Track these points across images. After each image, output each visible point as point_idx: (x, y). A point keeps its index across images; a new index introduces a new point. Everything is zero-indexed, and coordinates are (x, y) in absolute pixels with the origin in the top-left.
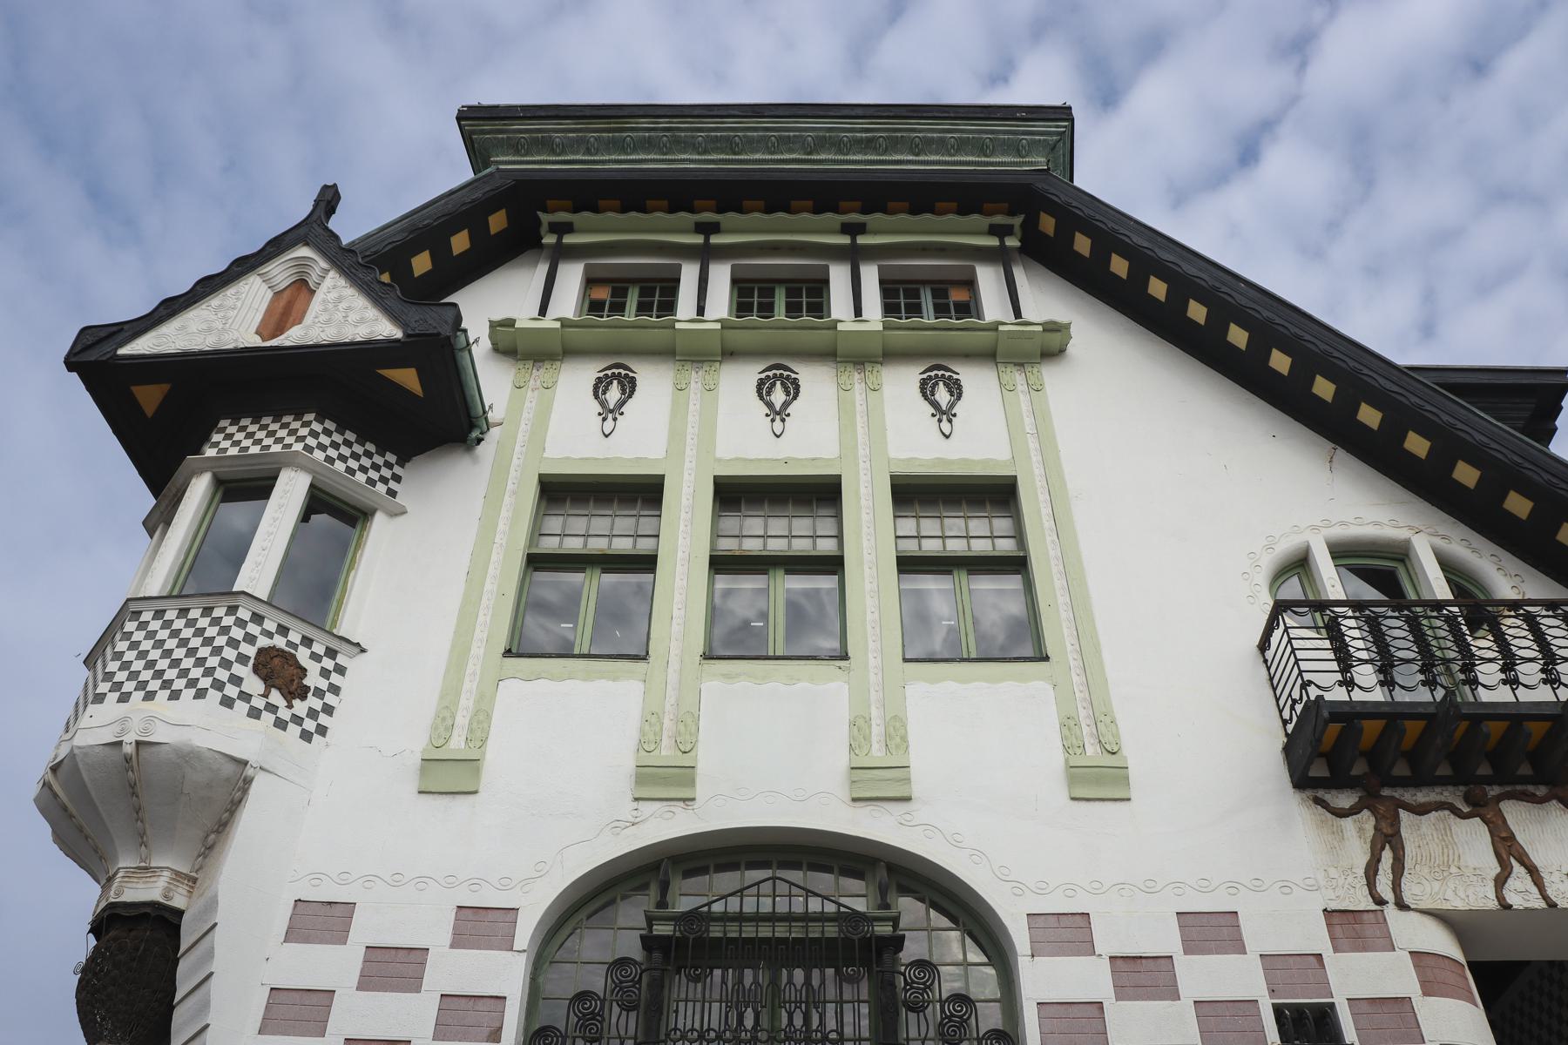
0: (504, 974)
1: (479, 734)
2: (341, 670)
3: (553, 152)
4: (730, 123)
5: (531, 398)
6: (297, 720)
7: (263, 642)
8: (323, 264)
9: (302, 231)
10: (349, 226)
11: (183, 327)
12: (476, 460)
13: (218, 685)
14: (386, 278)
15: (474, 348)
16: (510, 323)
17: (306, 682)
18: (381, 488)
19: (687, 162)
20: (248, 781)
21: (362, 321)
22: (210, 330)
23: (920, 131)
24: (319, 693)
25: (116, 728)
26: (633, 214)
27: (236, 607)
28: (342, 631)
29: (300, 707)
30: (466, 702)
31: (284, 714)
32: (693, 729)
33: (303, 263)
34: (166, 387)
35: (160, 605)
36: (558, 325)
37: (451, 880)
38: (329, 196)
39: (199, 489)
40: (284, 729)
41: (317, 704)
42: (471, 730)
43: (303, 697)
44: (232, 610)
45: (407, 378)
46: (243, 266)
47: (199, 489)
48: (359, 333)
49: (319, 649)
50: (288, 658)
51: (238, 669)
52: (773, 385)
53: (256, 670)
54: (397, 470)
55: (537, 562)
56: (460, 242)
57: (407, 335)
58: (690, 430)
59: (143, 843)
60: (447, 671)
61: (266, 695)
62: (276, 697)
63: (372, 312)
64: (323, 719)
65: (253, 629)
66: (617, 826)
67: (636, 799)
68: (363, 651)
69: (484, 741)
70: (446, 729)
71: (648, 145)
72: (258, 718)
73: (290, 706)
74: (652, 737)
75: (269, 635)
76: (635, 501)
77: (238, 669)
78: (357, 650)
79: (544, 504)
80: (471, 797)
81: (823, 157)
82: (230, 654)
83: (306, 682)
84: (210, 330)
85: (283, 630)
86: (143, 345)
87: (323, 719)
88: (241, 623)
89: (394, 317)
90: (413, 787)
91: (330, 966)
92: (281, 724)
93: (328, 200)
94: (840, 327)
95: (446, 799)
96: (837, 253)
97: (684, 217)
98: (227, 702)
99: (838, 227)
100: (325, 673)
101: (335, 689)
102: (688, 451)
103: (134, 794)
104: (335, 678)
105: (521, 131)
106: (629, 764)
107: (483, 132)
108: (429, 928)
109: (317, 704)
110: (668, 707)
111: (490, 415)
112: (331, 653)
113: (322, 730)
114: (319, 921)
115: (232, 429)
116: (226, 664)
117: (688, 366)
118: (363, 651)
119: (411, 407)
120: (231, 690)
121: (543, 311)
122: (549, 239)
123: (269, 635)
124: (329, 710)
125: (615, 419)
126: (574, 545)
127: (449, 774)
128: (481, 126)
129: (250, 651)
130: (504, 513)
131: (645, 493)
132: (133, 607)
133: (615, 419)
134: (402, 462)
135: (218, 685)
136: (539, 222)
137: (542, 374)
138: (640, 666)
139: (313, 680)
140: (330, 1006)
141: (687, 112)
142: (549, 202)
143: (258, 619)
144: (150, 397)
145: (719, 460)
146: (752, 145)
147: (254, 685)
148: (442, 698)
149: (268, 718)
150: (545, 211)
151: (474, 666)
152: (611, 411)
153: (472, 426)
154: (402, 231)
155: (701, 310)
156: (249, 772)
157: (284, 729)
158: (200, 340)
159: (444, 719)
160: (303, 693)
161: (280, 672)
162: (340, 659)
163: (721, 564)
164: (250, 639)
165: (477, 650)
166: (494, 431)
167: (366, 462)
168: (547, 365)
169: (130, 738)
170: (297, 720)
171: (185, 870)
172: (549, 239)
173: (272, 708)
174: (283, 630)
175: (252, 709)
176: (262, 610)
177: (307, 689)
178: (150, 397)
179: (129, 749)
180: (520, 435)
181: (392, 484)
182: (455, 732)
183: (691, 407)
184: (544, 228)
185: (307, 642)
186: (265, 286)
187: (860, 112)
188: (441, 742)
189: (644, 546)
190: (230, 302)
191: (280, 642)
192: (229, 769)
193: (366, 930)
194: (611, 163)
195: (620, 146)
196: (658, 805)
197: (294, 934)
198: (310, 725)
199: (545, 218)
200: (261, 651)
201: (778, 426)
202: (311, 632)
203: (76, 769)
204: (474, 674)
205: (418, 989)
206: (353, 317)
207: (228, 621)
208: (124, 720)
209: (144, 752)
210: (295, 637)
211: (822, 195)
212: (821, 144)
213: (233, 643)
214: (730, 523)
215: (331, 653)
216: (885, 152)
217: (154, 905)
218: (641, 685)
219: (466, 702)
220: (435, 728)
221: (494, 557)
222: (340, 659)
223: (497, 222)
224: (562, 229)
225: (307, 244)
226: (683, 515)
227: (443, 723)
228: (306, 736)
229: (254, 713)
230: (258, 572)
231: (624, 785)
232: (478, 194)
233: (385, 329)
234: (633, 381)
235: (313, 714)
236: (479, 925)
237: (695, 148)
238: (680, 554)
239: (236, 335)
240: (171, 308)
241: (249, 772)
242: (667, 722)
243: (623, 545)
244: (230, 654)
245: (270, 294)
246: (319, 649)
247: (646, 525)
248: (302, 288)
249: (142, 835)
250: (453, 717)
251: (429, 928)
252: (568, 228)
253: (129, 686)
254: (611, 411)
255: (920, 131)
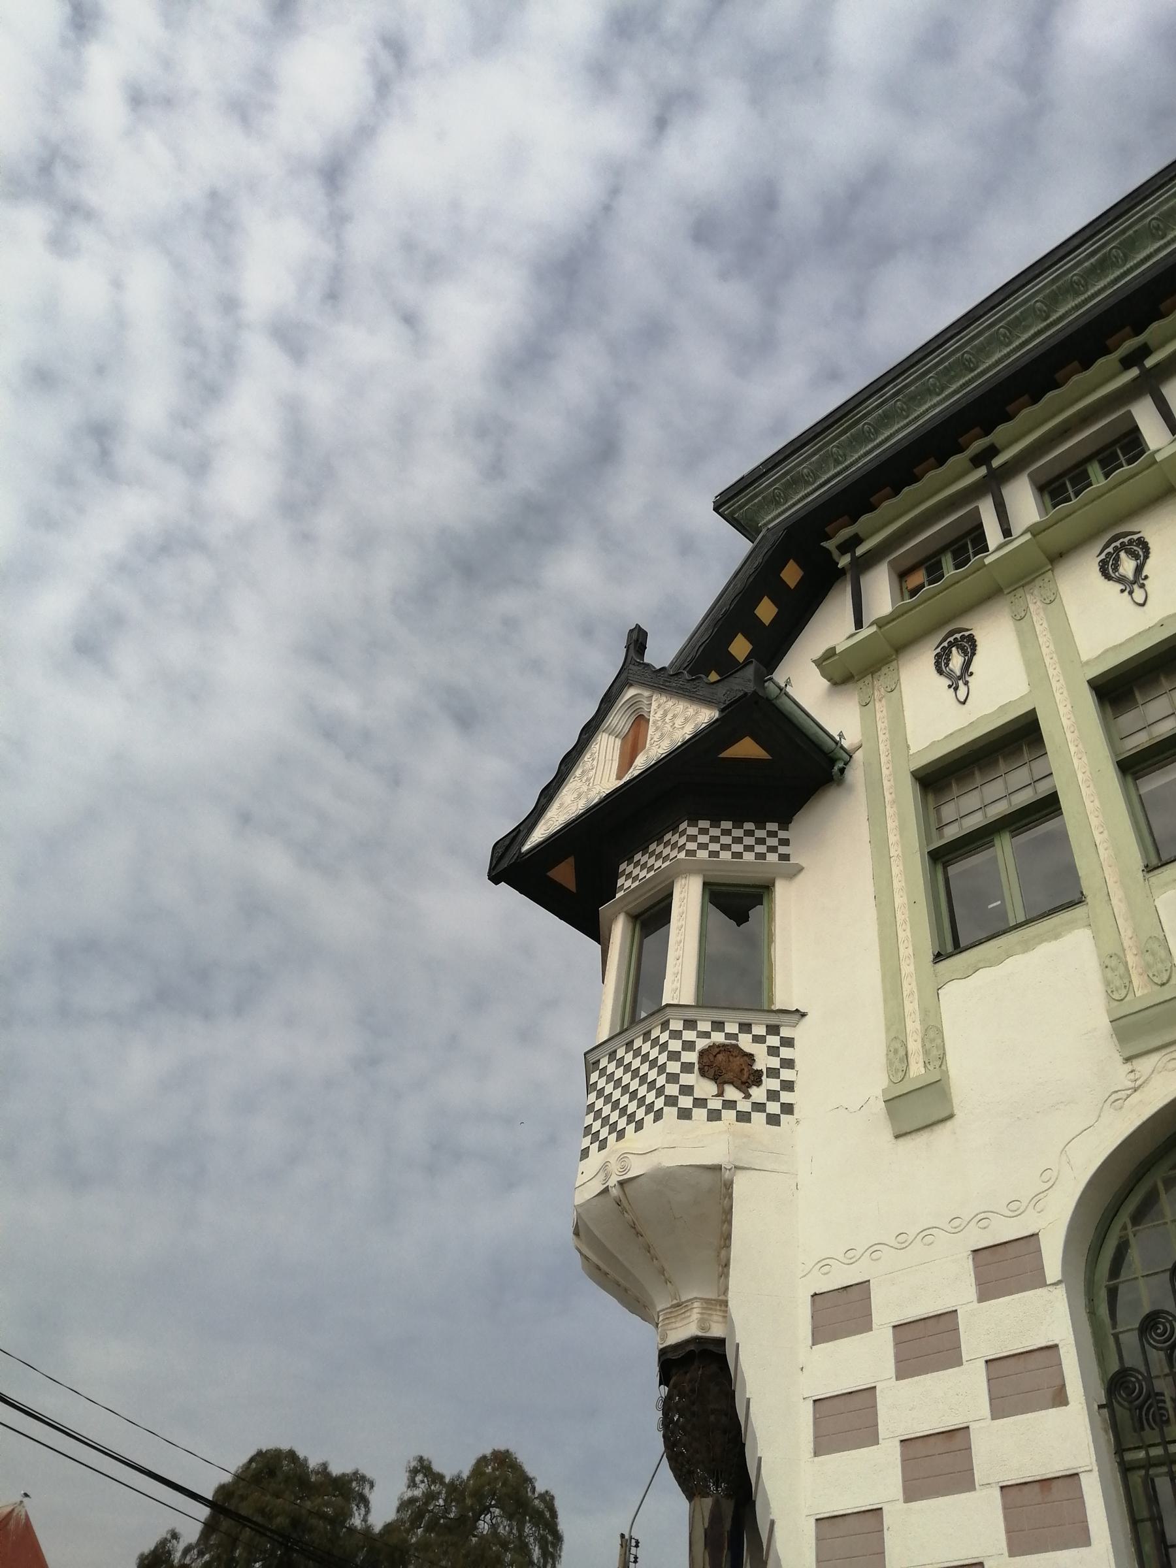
0: (1047, 1317)
1: (935, 1052)
2: (788, 1042)
3: (808, 483)
4: (951, 346)
5: (881, 709)
6: (759, 1107)
7: (702, 1044)
8: (646, 693)
9: (623, 676)
10: (662, 652)
11: (562, 805)
12: (850, 789)
13: (671, 1101)
14: (714, 677)
15: (789, 689)
16: (831, 653)
17: (757, 1066)
18: (772, 858)
19: (932, 409)
20: (729, 1185)
21: (687, 720)
22: (579, 797)
23: (1152, 212)
24: (773, 1073)
25: (601, 1176)
26: (906, 489)
27: (668, 1021)
28: (778, 1005)
29: (758, 1094)
30: (913, 1025)
31: (744, 1106)
32: (1162, 953)
33: (634, 702)
34: (571, 860)
35: (609, 1048)
36: (874, 629)
37: (956, 1222)
38: (635, 636)
39: (619, 931)
40: (749, 1121)
41: (773, 1084)
42: (926, 1052)
43: (758, 1082)
44: (665, 1025)
45: (747, 748)
46: (589, 732)
47: (619, 931)
48: (684, 732)
49: (759, 1030)
50: (731, 1050)
51: (687, 1079)
52: (1118, 556)
53: (703, 1073)
54: (782, 834)
55: (941, 857)
56: (766, 611)
57: (722, 711)
58: (1044, 650)
59: (667, 1281)
60: (885, 1001)
61: (720, 1094)
62: (732, 1093)
63: (691, 709)
64: (786, 1097)
65: (689, 1035)
66: (1116, 1099)
67: (1128, 1060)
68: (804, 1015)
69: (942, 1058)
70: (901, 1061)
71: (887, 419)
72: (719, 1119)
73: (748, 1096)
74: (1118, 983)
75: (707, 1035)
76: (1020, 749)
77: (687, 1079)
78: (796, 1017)
79: (931, 798)
80: (949, 1124)
81: (1061, 311)
82: (674, 1067)
83: (757, 1066)
84: (579, 797)
85: (718, 1026)
86: (539, 834)
87: (786, 1097)
88: (676, 1035)
89: (707, 701)
90: (887, 1134)
91: (864, 1359)
92: (743, 1117)
93: (637, 641)
94: (1159, 457)
95: (924, 1137)
96: (1130, 394)
97: (957, 461)
98: (685, 1114)
99: (1118, 365)
100: (773, 1051)
101: (789, 1064)
102: (1051, 672)
103: (638, 1234)
104: (785, 1053)
105: (770, 485)
106: (1103, 1022)
107: (741, 507)
108: (948, 1285)
109: (774, 1084)
110: (1127, 943)
111: (843, 742)
112: (773, 1030)
113: (788, 1109)
114: (841, 1312)
115: (630, 869)
116: (673, 1078)
117: (1020, 592)
118: (804, 1015)
119: (764, 774)
120: (686, 1102)
121: (859, 624)
122: (844, 561)
123: (707, 1035)
124: (788, 1086)
125: (966, 683)
126: (975, 822)
127: (918, 1107)
128: (732, 504)
129: (691, 1057)
130: (892, 824)
131: (1021, 737)
132: (592, 1058)
133: (966, 683)
134: (784, 825)
135: (671, 1101)
136: (828, 552)
137: (881, 682)
138: (1078, 912)
139: (763, 1061)
140: (875, 1406)
141: (906, 365)
142: (827, 529)
143: (690, 1024)
144: (564, 874)
145: (1087, 663)
146: (983, 351)
147: (705, 1088)
148: (888, 1030)
149: (729, 1115)
150: (828, 538)
151: (909, 986)
152: (960, 678)
153: (832, 761)
154: (707, 630)
155: (1007, 532)
156: (727, 1175)
157: (749, 1121)
158: (574, 809)
159: (896, 1051)
160: (756, 1079)
161: (728, 1067)
162: (785, 1032)
163: (1132, 767)
164: (689, 1046)
165: (908, 968)
166: (858, 756)
167: (749, 841)
168: (885, 670)
169: (613, 1181)
170: (759, 1107)
171: (713, 1296)
172: (844, 561)
173: (730, 1104)
174: (718, 1026)
175: (711, 1112)
176: (690, 1015)
177: (759, 1073)
178: (564, 874)
179: (615, 1192)
180: (882, 747)
181: (783, 850)
182: (912, 1060)
183: (1038, 628)
184: (836, 554)
185: (745, 1027)
186: (612, 738)
187: (1076, 242)
188: (901, 1074)
189: (1043, 789)
190: (588, 766)
191: (718, 1038)
192: (707, 1179)
193: (889, 1308)
194: (862, 458)
195: (862, 438)
196: (1154, 1058)
197: (822, 1332)
198: (773, 1108)
199: (830, 545)
200: (702, 1054)
201: (1139, 595)
202: (746, 1017)
203: (588, 1230)
204: (912, 993)
205: (959, 1362)
206: (679, 722)
207: (665, 1037)
208: (605, 1165)
209: (628, 1188)
210: (732, 1028)
211: (1082, 346)
212: (1054, 300)
213: (674, 1056)
214: (1128, 720)
215: (773, 1030)
216: (1126, 259)
217: (696, 1340)
218: (1087, 932)
219: (913, 1025)
220: (890, 1063)
221: (895, 870)
222: (785, 1032)
223: (791, 574)
224: (848, 546)
225: (631, 685)
226: (1069, 736)
227: (898, 1056)
228: (773, 1120)
229: (714, 1116)
230: (680, 982)
231: (1107, 1049)
232: (760, 560)
233: (705, 716)
234: (971, 640)
235: (773, 1095)
236: (1003, 1267)
237: (930, 392)
238: (1080, 776)
239: (598, 788)
240: (549, 794)
241: (727, 1175)
242: (1131, 959)
243: (1024, 798)
244: (674, 1067)
245: (618, 742)
246: (759, 1030)
247: (1038, 767)
248: (640, 721)
249: (662, 1271)
250: (905, 1045)
251: (948, 1285)
252: (857, 540)
253: (604, 1133)
254: (960, 678)
255: (1152, 212)
